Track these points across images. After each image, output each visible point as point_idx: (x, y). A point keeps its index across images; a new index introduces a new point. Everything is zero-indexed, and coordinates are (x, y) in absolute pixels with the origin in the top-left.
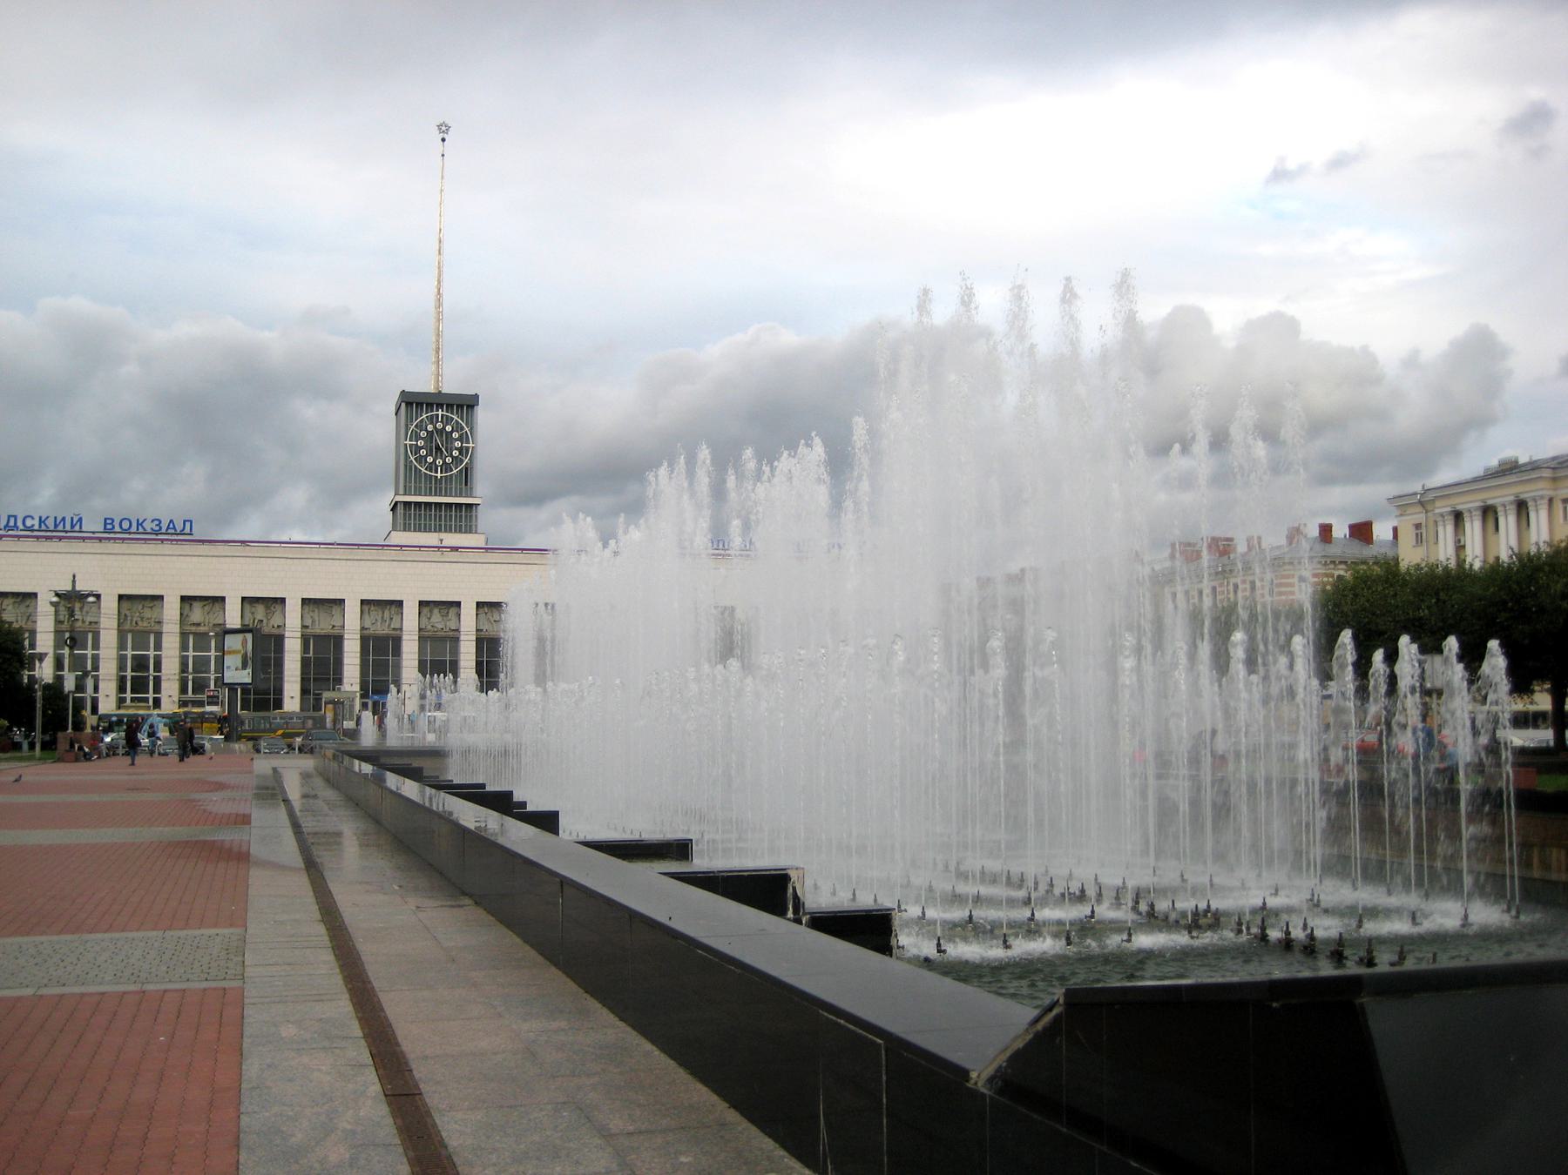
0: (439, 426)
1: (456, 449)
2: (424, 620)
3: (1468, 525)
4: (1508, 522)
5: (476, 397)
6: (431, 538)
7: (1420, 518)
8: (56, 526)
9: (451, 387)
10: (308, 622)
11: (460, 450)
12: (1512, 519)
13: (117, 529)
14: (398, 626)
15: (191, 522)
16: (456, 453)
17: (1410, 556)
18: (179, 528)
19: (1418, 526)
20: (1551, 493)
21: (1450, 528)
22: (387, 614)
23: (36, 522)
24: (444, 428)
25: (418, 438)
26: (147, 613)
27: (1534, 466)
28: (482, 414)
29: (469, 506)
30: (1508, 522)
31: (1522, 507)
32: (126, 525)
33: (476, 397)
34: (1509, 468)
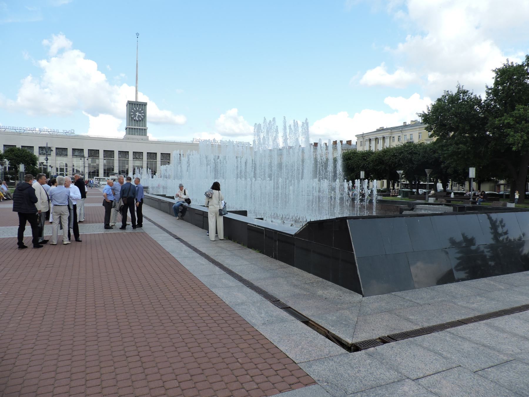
2: (134, 156)
3: (372, 142)
4: (381, 142)
5: (146, 103)
7: (362, 140)
10: (105, 156)
12: (382, 141)
14: (128, 157)
17: (360, 149)
19: (361, 142)
20: (390, 135)
21: (368, 142)
26: (63, 152)
27: (387, 129)
28: (148, 106)
29: (145, 129)
30: (381, 142)
31: (384, 138)
33: (146, 103)
34: (382, 130)
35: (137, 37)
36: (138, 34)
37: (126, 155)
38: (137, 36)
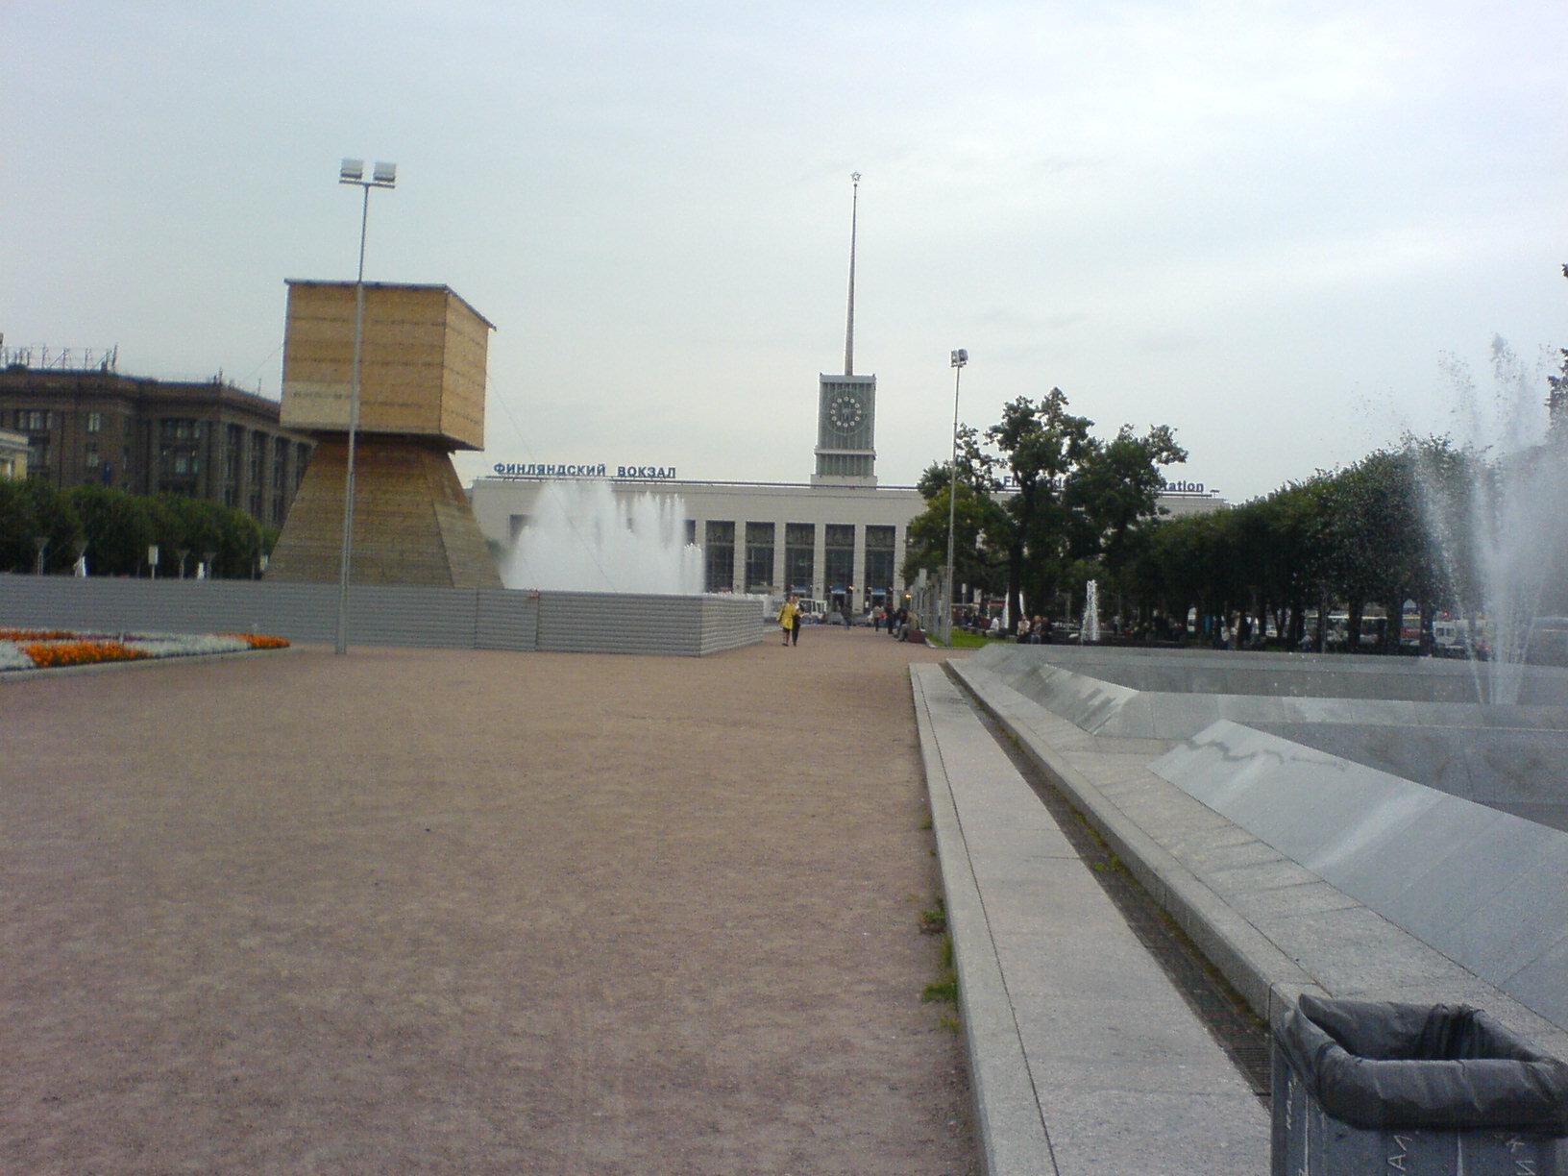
0: (846, 399)
1: (858, 415)
6: (837, 480)
8: (588, 474)
9: (858, 371)
11: (861, 416)
13: (627, 474)
15: (674, 469)
16: (857, 418)
18: (666, 473)
22: (804, 533)
23: (576, 470)
24: (849, 402)
25: (831, 408)
29: (866, 457)
32: (632, 472)
35: (856, 185)
36: (856, 177)
37: (807, 536)
38: (854, 183)
